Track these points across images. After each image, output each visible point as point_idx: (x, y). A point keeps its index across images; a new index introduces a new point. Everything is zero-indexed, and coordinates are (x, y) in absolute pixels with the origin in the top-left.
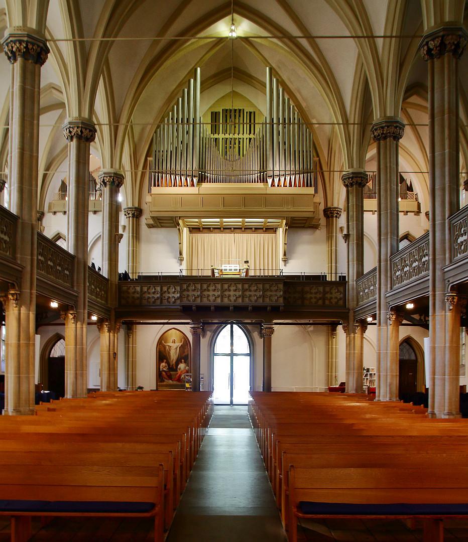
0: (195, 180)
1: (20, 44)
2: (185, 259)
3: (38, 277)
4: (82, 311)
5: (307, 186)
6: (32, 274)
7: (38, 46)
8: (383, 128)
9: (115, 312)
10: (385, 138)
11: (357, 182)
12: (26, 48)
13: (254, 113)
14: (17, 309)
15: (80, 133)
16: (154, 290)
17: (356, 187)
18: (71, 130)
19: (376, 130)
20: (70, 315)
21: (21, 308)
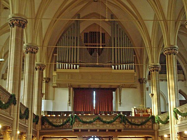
0: (78, 66)
1: (17, 21)
2: (71, 103)
3: (20, 123)
4: (29, 134)
5: (131, 69)
6: (17, 121)
7: (24, 22)
8: (169, 50)
9: (40, 132)
10: (170, 54)
11: (156, 69)
12: (19, 22)
13: (105, 34)
14: (10, 138)
15: (31, 50)
16: (59, 121)
17: (156, 72)
18: (28, 49)
19: (166, 51)
20: (24, 137)
21: (12, 138)
